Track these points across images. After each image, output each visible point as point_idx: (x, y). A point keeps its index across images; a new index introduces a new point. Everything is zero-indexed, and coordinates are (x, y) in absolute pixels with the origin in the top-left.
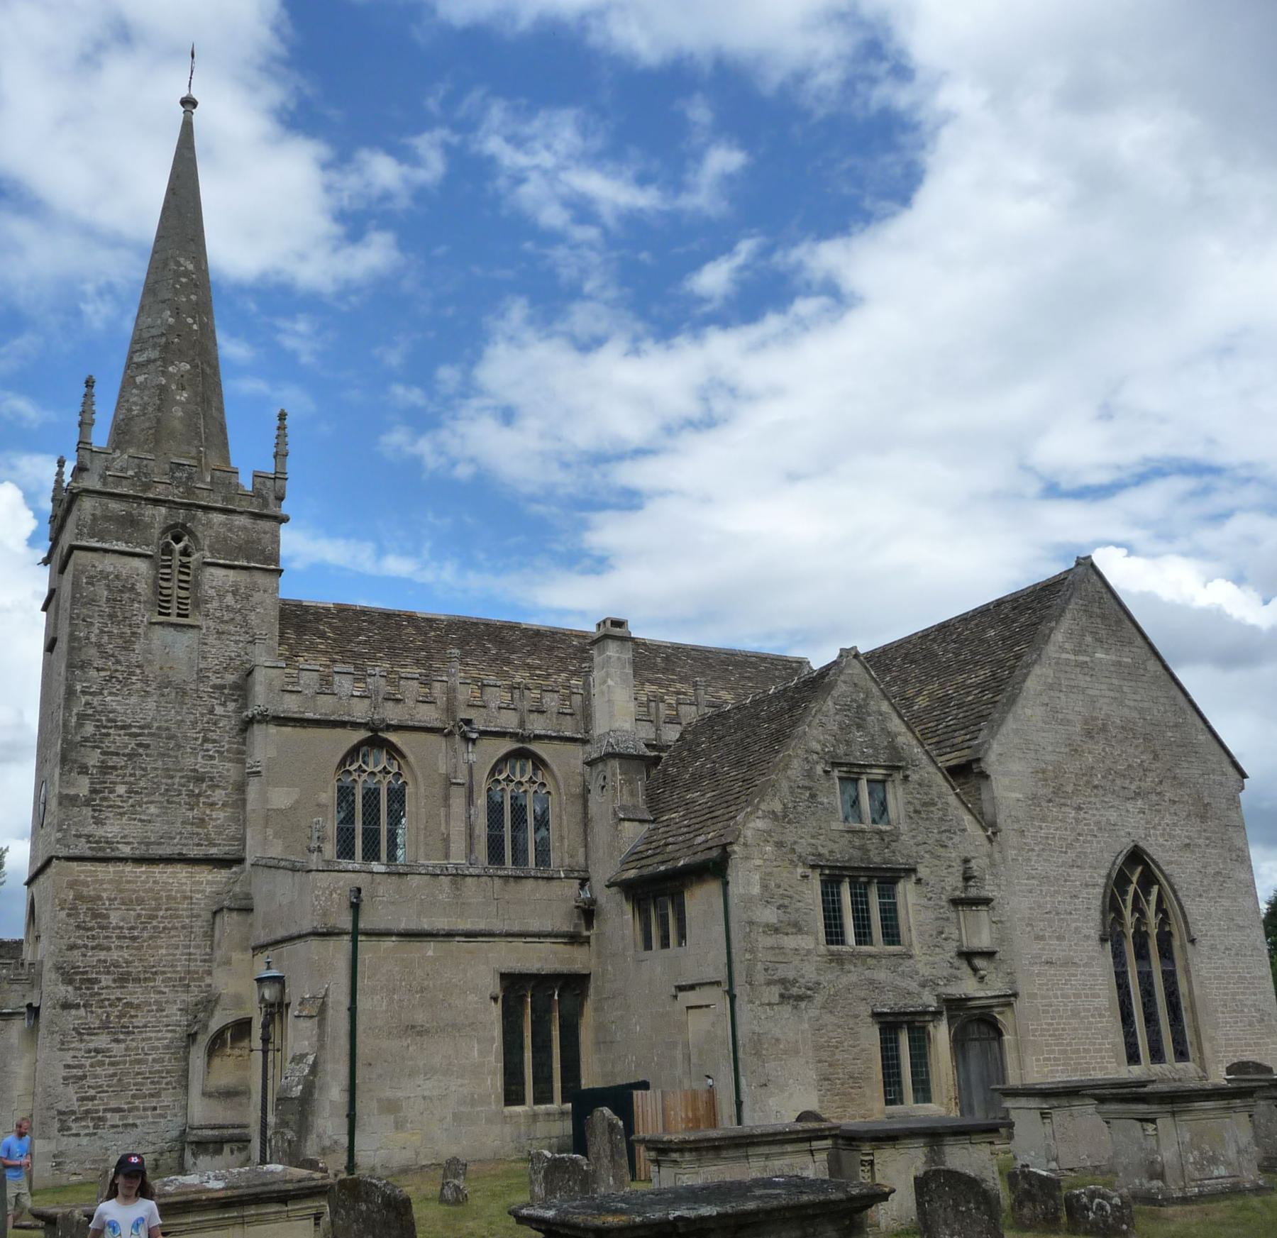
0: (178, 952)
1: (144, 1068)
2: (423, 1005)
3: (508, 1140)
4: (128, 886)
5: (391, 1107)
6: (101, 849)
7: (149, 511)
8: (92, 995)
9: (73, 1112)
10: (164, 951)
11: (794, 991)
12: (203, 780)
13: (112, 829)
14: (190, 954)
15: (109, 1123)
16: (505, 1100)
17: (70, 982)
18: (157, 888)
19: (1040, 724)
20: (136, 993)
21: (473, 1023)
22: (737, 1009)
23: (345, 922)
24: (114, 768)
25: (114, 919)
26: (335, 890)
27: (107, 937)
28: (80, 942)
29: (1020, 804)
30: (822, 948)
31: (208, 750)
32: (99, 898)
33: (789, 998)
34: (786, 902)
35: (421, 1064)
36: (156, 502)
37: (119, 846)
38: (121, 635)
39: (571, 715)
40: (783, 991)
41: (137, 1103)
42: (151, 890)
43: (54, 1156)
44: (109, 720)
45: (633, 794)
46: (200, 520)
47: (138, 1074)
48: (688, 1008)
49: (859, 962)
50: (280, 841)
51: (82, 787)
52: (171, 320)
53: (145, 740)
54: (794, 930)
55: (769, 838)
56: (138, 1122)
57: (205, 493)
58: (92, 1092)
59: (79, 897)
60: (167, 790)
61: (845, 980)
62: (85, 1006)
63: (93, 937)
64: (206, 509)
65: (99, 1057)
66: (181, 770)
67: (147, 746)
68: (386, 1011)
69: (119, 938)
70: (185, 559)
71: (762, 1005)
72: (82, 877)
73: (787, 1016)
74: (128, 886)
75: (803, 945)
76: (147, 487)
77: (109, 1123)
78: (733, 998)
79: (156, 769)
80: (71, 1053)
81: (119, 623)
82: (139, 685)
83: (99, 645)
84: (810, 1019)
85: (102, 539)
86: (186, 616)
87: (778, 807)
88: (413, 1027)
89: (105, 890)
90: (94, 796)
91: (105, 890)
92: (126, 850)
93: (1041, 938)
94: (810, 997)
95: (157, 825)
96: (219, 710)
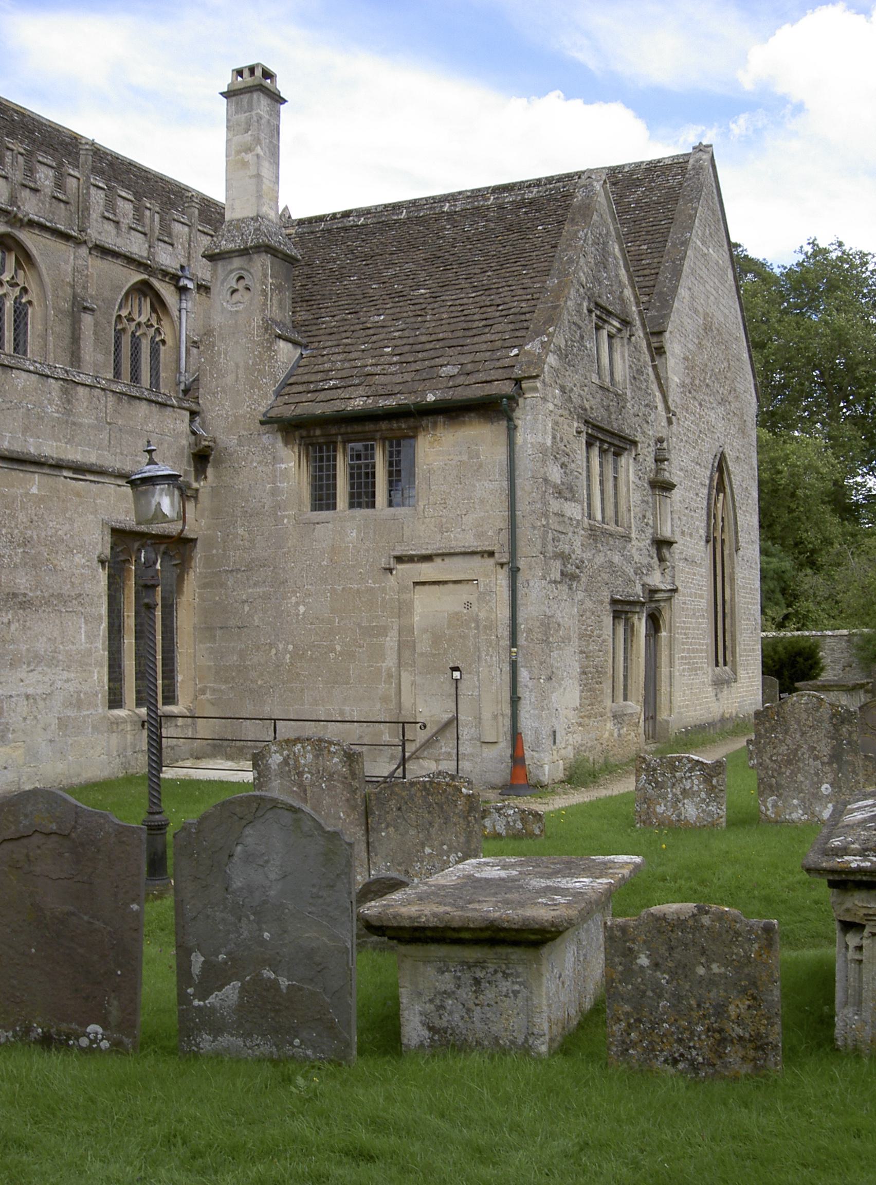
2: (26, 564)
3: (115, 754)
16: (110, 701)
21: (80, 595)
22: (519, 585)
35: (24, 648)
39: (66, 203)
45: (281, 307)
48: (416, 584)
78: (514, 572)
88: (15, 595)
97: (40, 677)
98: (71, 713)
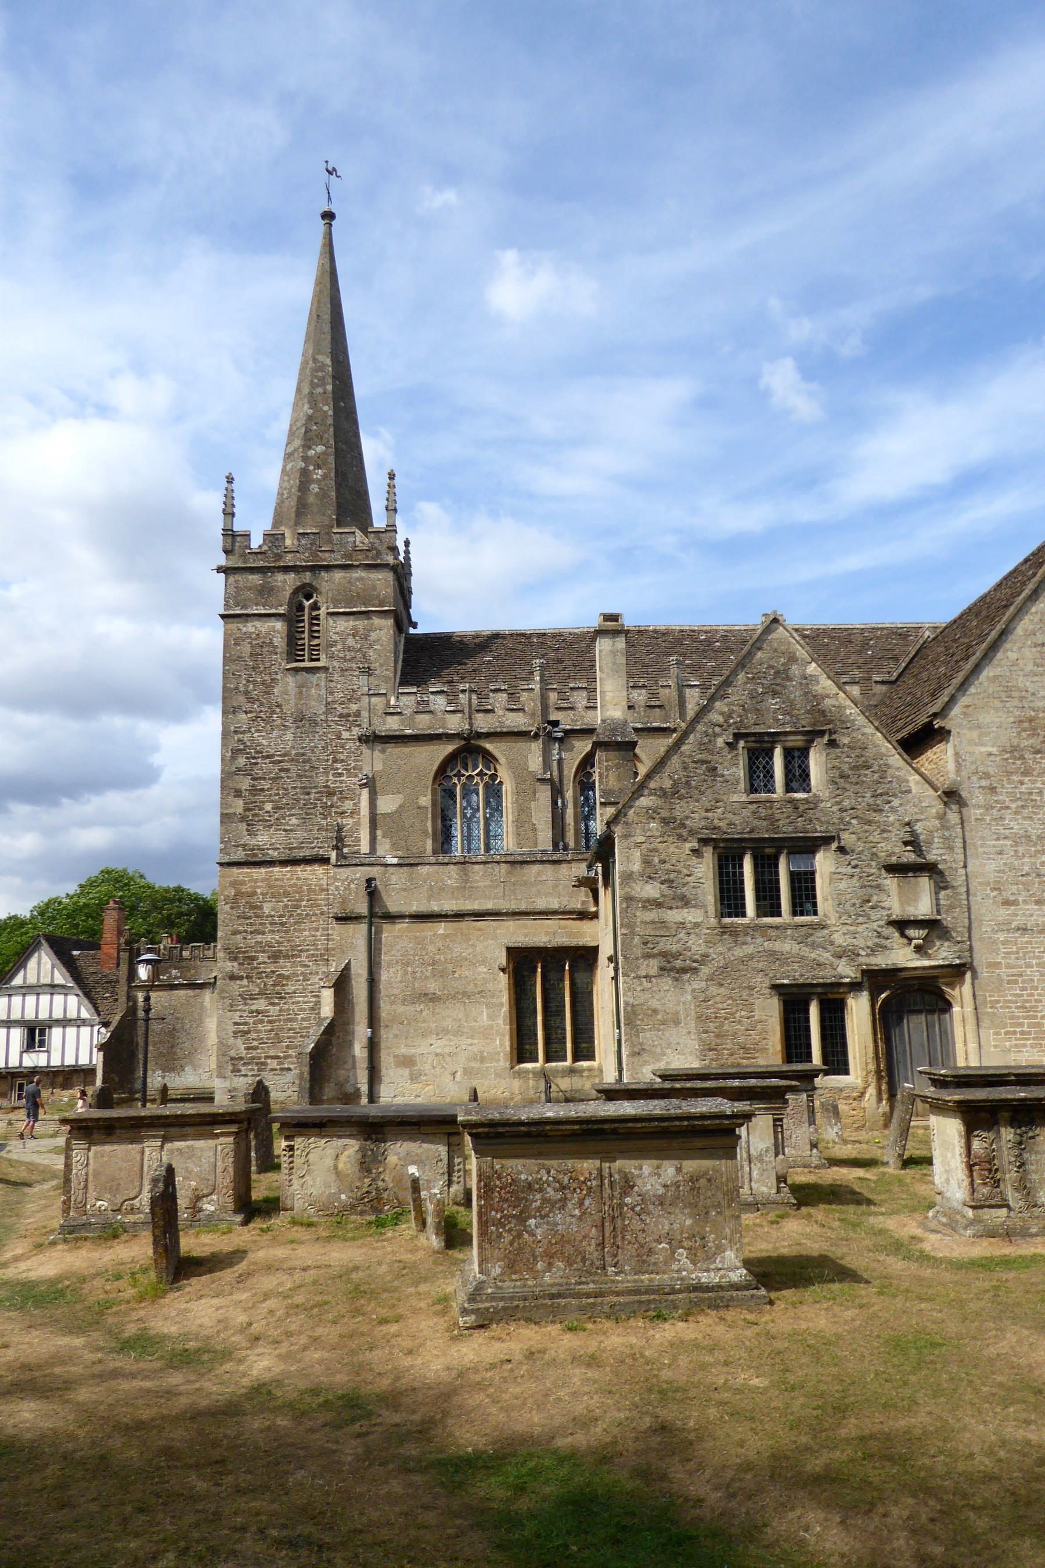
0: (318, 934)
1: (295, 1025)
4: (277, 883)
5: (407, 1062)
6: (255, 855)
7: (280, 577)
8: (252, 969)
9: (242, 1058)
10: (307, 933)
11: (678, 963)
12: (333, 794)
13: (263, 838)
14: (328, 935)
15: (269, 1067)
17: (235, 959)
18: (300, 883)
19: (1030, 667)
20: (285, 966)
23: (362, 908)
24: (262, 790)
25: (267, 909)
26: (352, 881)
27: (261, 924)
28: (241, 928)
29: (992, 758)
30: (713, 921)
31: (337, 769)
32: (255, 893)
33: (671, 970)
34: (672, 876)
36: (286, 569)
37: (270, 852)
38: (263, 683)
40: (663, 964)
41: (290, 1052)
42: (295, 885)
43: (230, 1091)
44: (257, 752)
46: (323, 578)
47: (290, 1029)
49: (757, 934)
50: (388, 840)
51: (238, 806)
52: (310, 412)
53: (285, 765)
54: (680, 904)
55: (655, 815)
56: (292, 1066)
57: (327, 555)
58: (255, 1043)
59: (239, 894)
60: (305, 804)
61: (739, 952)
62: (247, 977)
63: (251, 924)
64: (328, 568)
65: (260, 1016)
66: (315, 787)
67: (288, 770)
68: (401, 982)
69: (271, 924)
70: (314, 613)
71: (638, 977)
72: (241, 878)
73: (666, 988)
74: (277, 883)
75: (690, 918)
76: (278, 557)
77: (269, 1067)
79: (295, 788)
80: (239, 1013)
81: (261, 672)
82: (279, 721)
83: (246, 693)
84: (694, 991)
85: (244, 607)
86: (318, 660)
87: (667, 784)
88: (426, 995)
89: (259, 887)
90: (247, 813)
91: (259, 887)
92: (274, 854)
93: (1015, 903)
94: (696, 969)
95: (300, 834)
96: (345, 735)
97: (447, 1043)
98: (475, 1065)
